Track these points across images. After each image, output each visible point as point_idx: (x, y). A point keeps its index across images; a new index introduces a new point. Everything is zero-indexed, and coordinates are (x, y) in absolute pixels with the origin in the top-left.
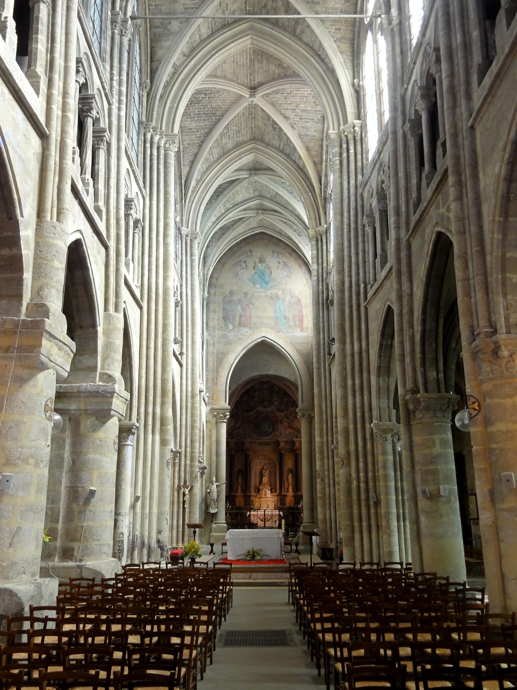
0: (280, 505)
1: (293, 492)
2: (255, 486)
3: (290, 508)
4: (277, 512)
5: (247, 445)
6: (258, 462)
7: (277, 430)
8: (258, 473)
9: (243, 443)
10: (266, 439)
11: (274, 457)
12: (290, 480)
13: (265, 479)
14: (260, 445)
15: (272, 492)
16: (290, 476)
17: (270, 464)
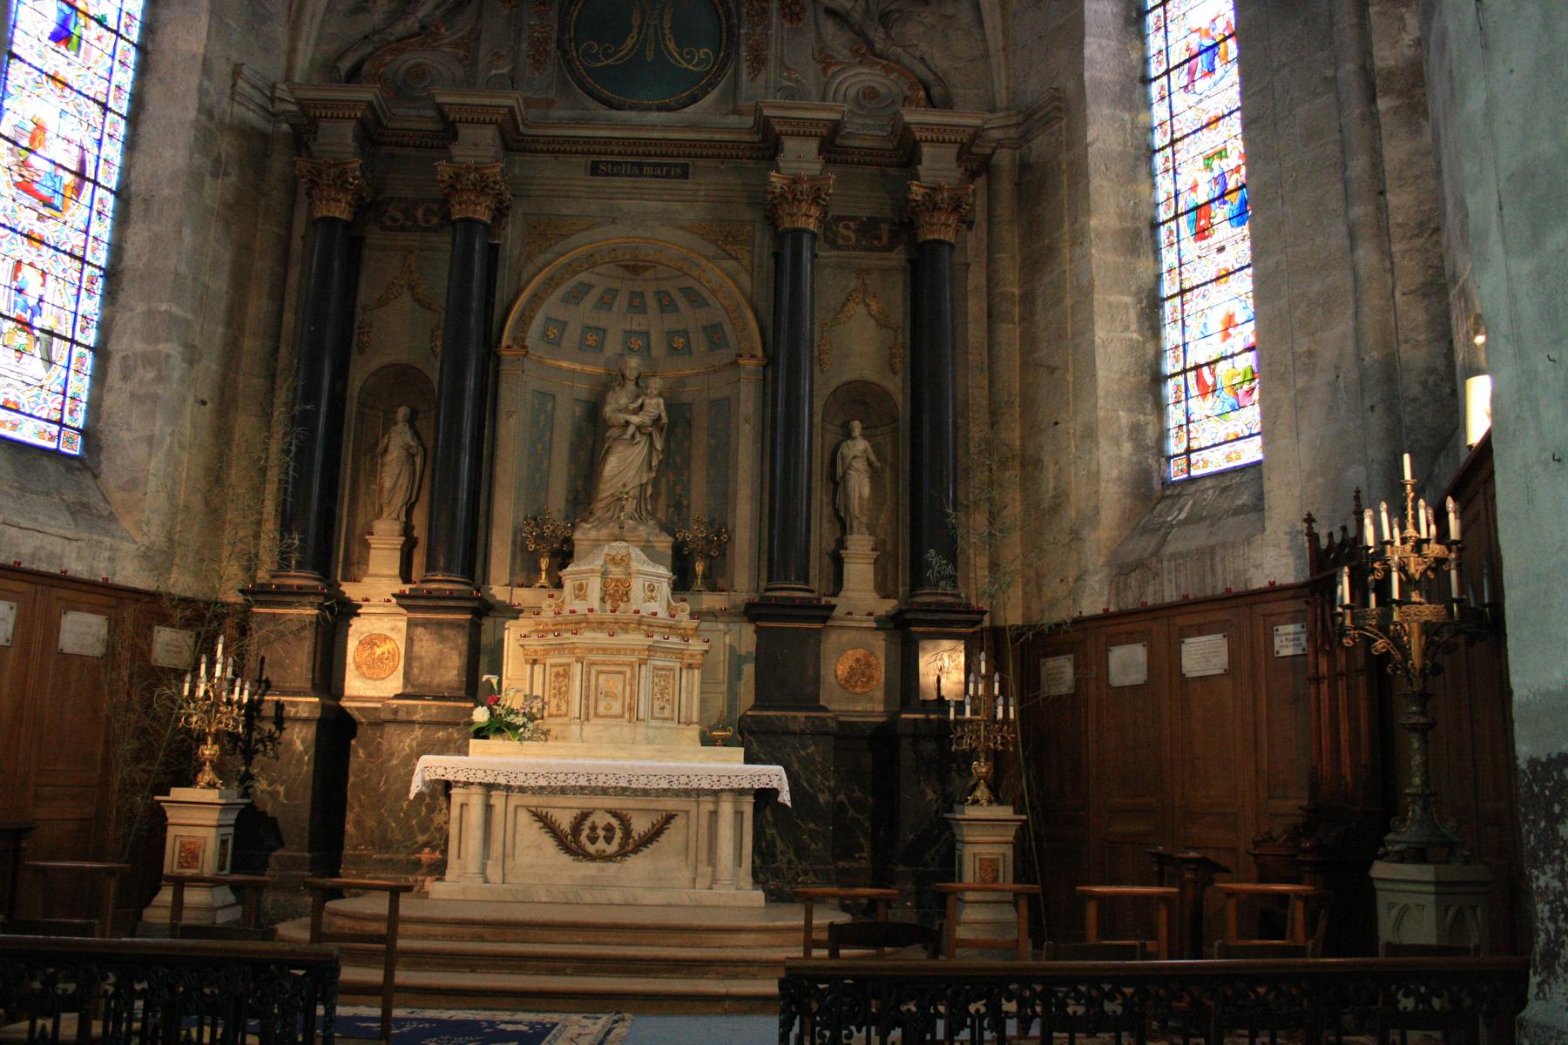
0: (761, 700)
1: (883, 590)
2: (537, 519)
3: (847, 736)
4: (729, 765)
5: (477, 147)
6: (581, 315)
7: (758, 62)
8: (566, 415)
9: (447, 130)
10: (654, 124)
11: (731, 284)
12: (860, 485)
13: (624, 467)
14: (595, 170)
15: (682, 583)
16: (859, 446)
17: (678, 344)
